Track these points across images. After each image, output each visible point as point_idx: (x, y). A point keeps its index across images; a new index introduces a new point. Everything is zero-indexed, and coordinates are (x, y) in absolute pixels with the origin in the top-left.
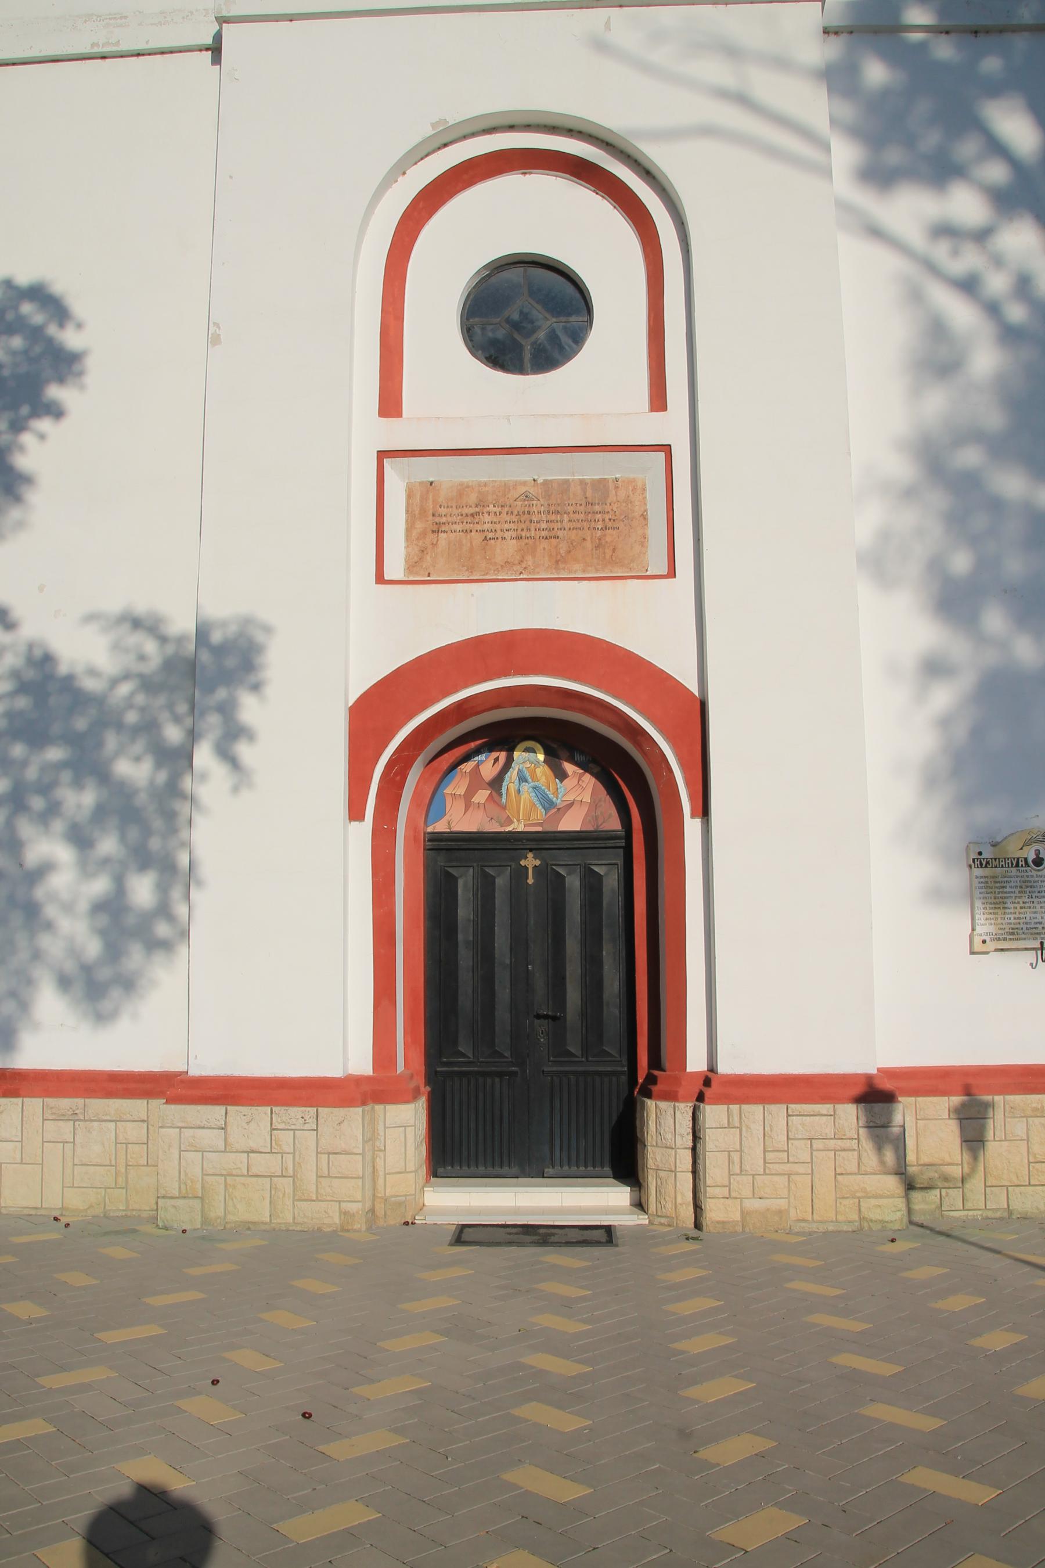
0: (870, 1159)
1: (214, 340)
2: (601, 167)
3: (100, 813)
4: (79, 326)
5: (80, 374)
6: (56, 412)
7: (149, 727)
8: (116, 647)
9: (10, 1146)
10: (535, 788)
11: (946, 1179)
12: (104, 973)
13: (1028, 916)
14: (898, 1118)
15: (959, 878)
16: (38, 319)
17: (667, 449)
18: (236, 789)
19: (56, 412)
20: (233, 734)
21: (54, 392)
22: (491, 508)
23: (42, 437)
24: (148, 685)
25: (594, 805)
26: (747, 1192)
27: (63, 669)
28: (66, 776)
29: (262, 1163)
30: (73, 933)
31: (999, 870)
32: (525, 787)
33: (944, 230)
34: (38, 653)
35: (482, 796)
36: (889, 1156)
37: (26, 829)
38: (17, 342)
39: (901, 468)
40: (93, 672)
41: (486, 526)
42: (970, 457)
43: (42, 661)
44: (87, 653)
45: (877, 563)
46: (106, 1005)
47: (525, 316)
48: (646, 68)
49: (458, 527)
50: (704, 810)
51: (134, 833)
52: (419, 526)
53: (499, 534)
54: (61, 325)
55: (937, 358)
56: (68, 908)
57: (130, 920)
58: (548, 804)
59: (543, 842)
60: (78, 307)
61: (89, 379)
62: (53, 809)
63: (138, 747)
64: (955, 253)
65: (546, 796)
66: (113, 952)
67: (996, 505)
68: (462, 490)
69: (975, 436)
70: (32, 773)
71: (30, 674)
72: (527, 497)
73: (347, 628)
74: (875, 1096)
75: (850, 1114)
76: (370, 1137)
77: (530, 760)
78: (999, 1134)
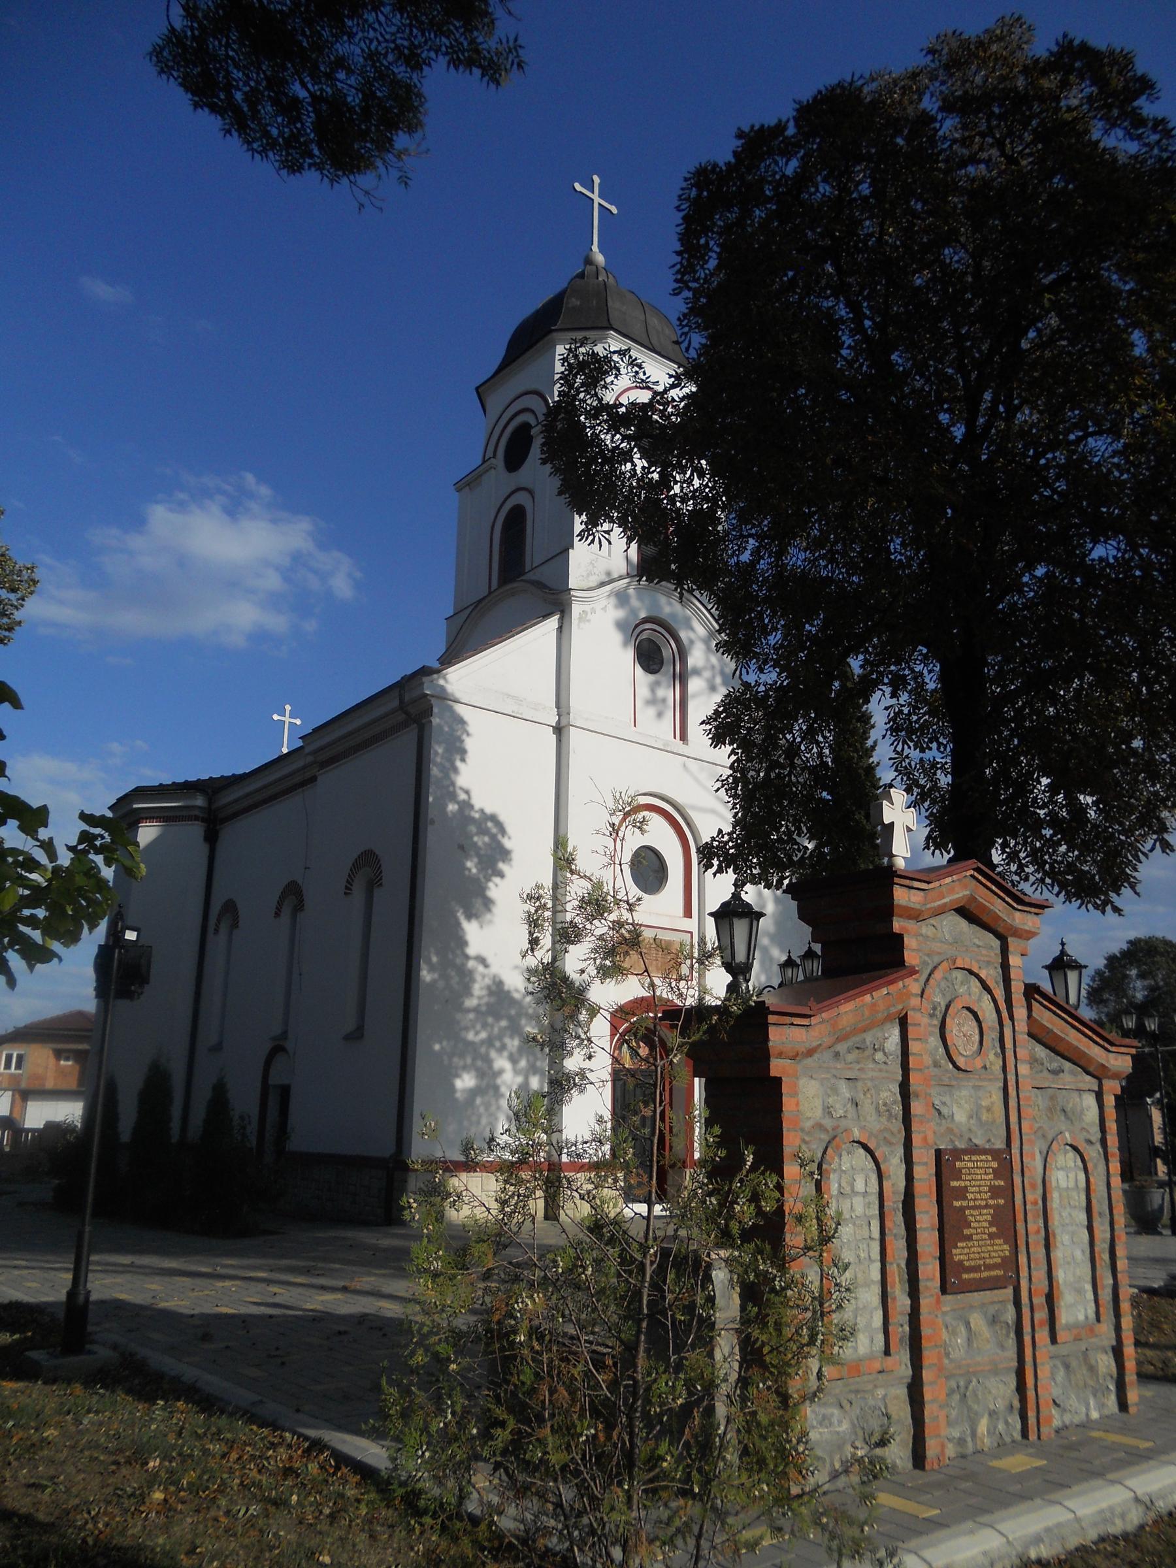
6: (501, 875)
16: (494, 830)
19: (501, 875)
21: (501, 865)
27: (506, 988)
28: (508, 1033)
38: (486, 839)
40: (517, 991)
61: (514, 863)
62: (503, 1047)
70: (496, 1030)
71: (494, 988)
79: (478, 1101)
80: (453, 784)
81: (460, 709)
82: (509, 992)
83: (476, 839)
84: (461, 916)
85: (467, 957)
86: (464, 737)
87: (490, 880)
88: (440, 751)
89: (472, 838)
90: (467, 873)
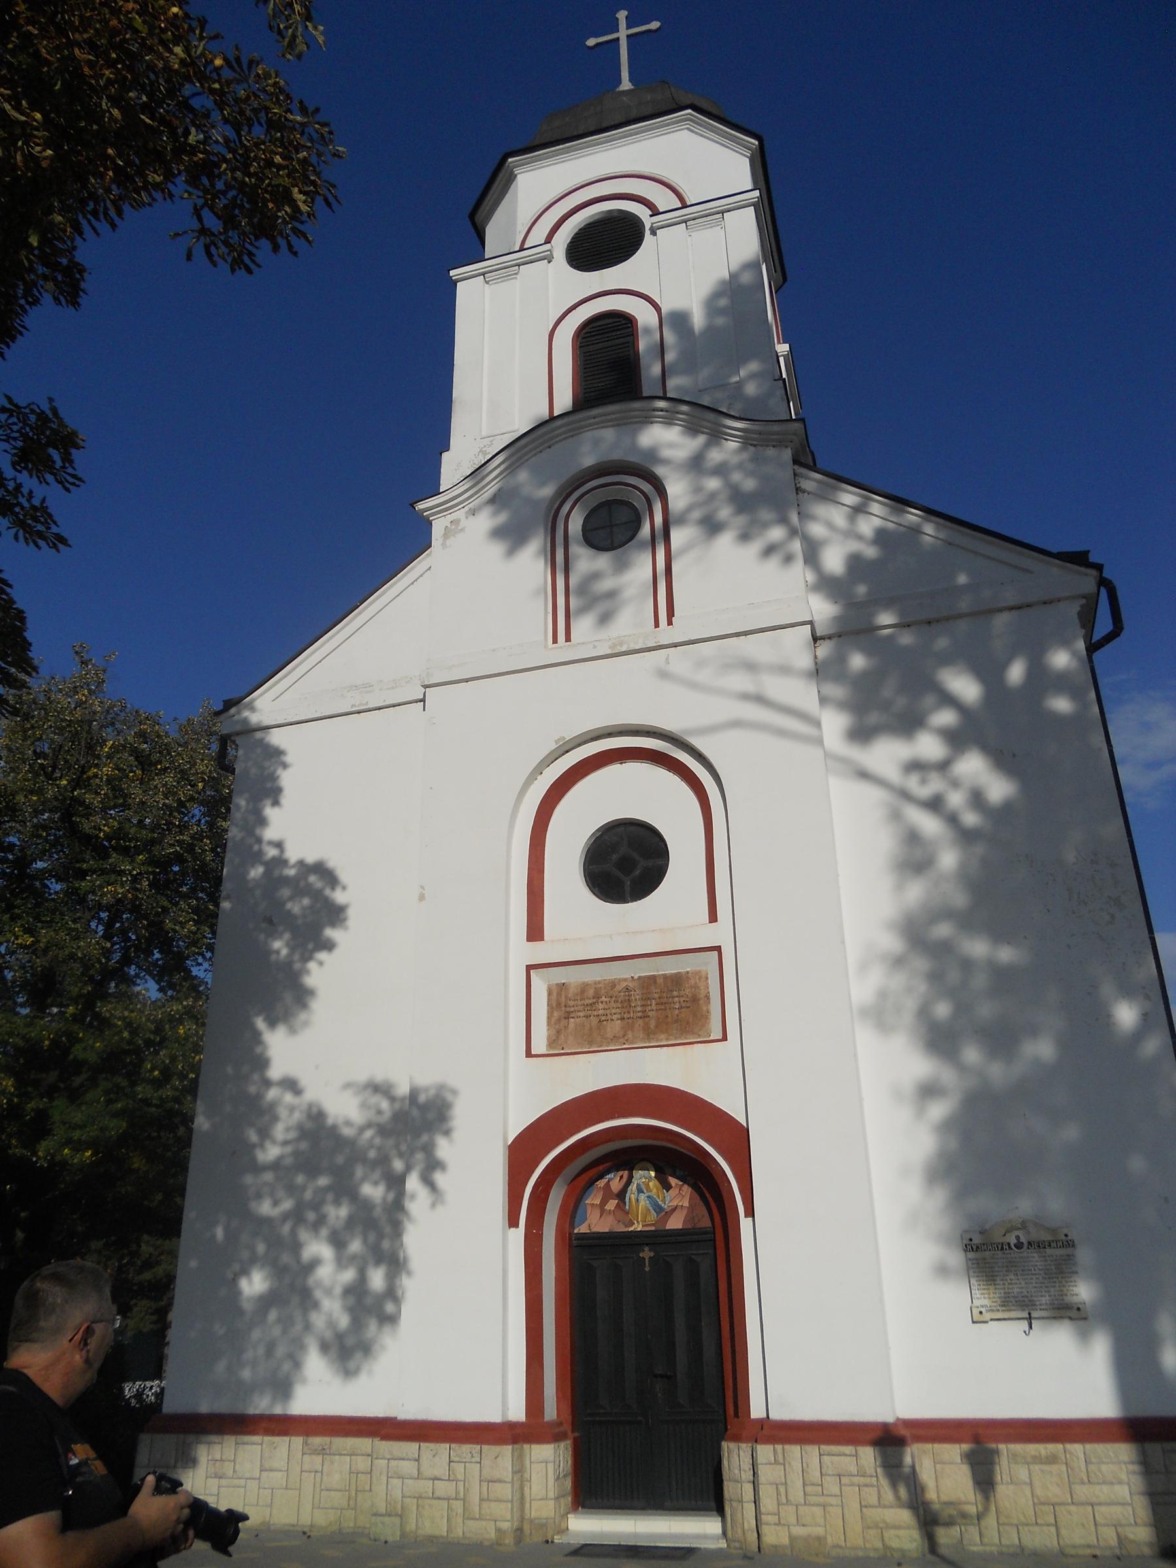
0: (888, 1495)
1: (422, 898)
2: (670, 754)
3: (351, 1223)
4: (344, 888)
5: (345, 920)
6: (329, 946)
7: (383, 1161)
8: (364, 1105)
9: (279, 1474)
10: (648, 1197)
11: (964, 1515)
12: (350, 1341)
13: (1016, 1290)
14: (908, 1460)
15: (956, 1258)
17: (718, 949)
18: (433, 1205)
19: (329, 946)
20: (433, 1165)
21: (329, 932)
22: (604, 999)
23: (321, 963)
24: (382, 1131)
25: (691, 1208)
26: (793, 1520)
28: (330, 1197)
29: (444, 1488)
30: (332, 1310)
31: (987, 1253)
32: (642, 1197)
33: (915, 766)
34: (315, 1110)
35: (612, 1204)
36: (903, 1492)
37: (304, 1235)
38: (306, 901)
39: (891, 943)
40: (348, 1123)
41: (601, 1012)
42: (943, 930)
43: (317, 1116)
44: (345, 1110)
45: (878, 1015)
46: (352, 1365)
47: (626, 862)
48: (693, 685)
49: (581, 1014)
50: (750, 1212)
51: (372, 1237)
52: (556, 1014)
53: (609, 1017)
54: (333, 889)
55: (914, 858)
56: (329, 1292)
57: (369, 1301)
58: (658, 1209)
59: (658, 1239)
60: (343, 876)
61: (351, 923)
62: (321, 1220)
63: (377, 1175)
64: (923, 782)
65: (651, 1202)
66: (357, 1323)
67: (967, 965)
68: (584, 988)
69: (947, 914)
70: (308, 1195)
71: (309, 1125)
72: (627, 989)
73: (508, 1087)
74: (889, 1439)
75: (868, 1455)
76: (519, 1469)
77: (645, 1177)
78: (1006, 1478)
79: (273, 1315)
80: (259, 840)
81: (276, 738)
82: (334, 1128)
83: (289, 906)
84: (260, 1024)
85: (268, 1083)
86: (280, 771)
87: (310, 958)
88: (243, 803)
89: (283, 904)
90: (274, 957)
